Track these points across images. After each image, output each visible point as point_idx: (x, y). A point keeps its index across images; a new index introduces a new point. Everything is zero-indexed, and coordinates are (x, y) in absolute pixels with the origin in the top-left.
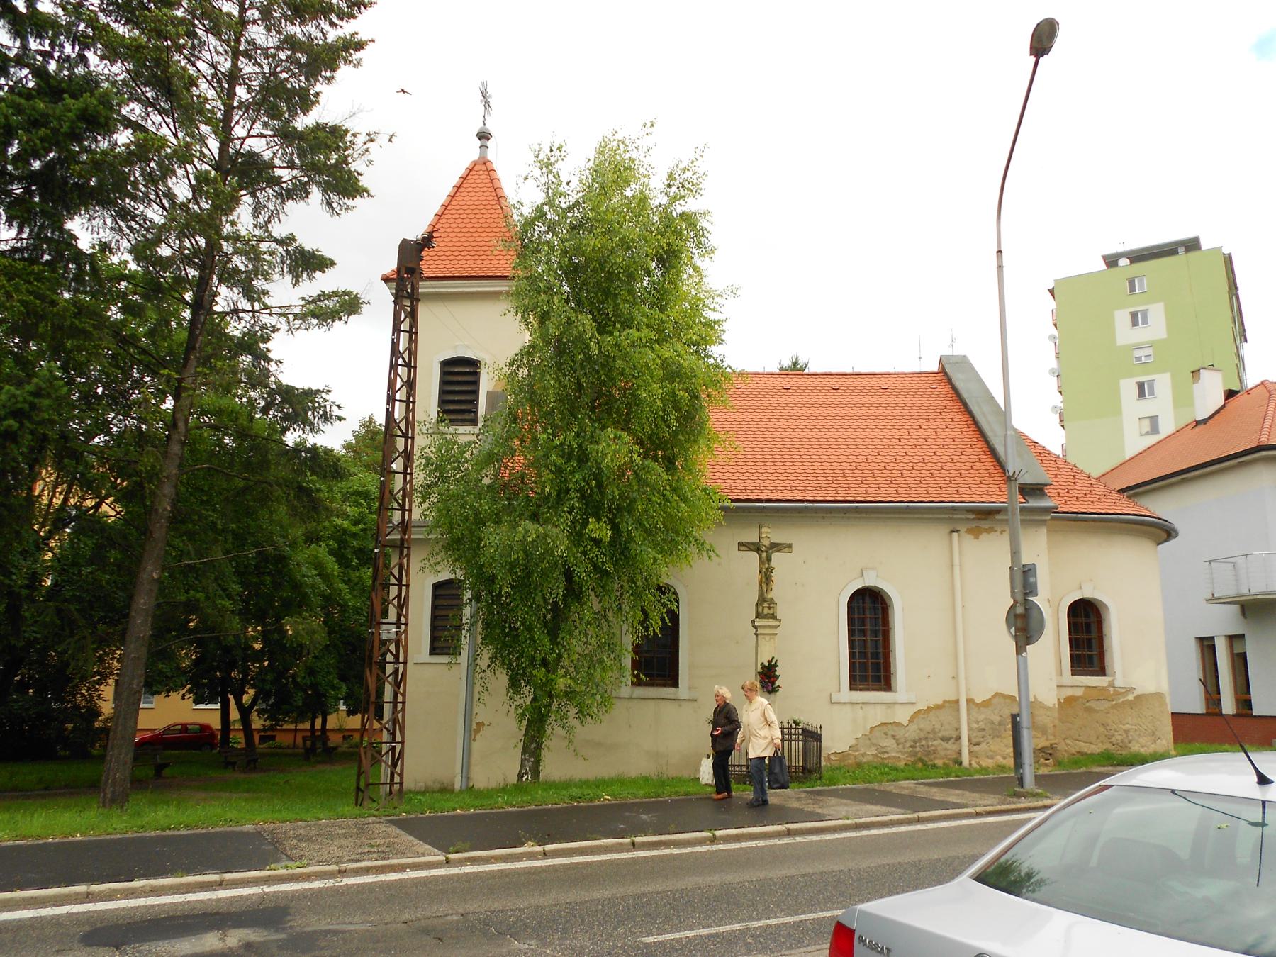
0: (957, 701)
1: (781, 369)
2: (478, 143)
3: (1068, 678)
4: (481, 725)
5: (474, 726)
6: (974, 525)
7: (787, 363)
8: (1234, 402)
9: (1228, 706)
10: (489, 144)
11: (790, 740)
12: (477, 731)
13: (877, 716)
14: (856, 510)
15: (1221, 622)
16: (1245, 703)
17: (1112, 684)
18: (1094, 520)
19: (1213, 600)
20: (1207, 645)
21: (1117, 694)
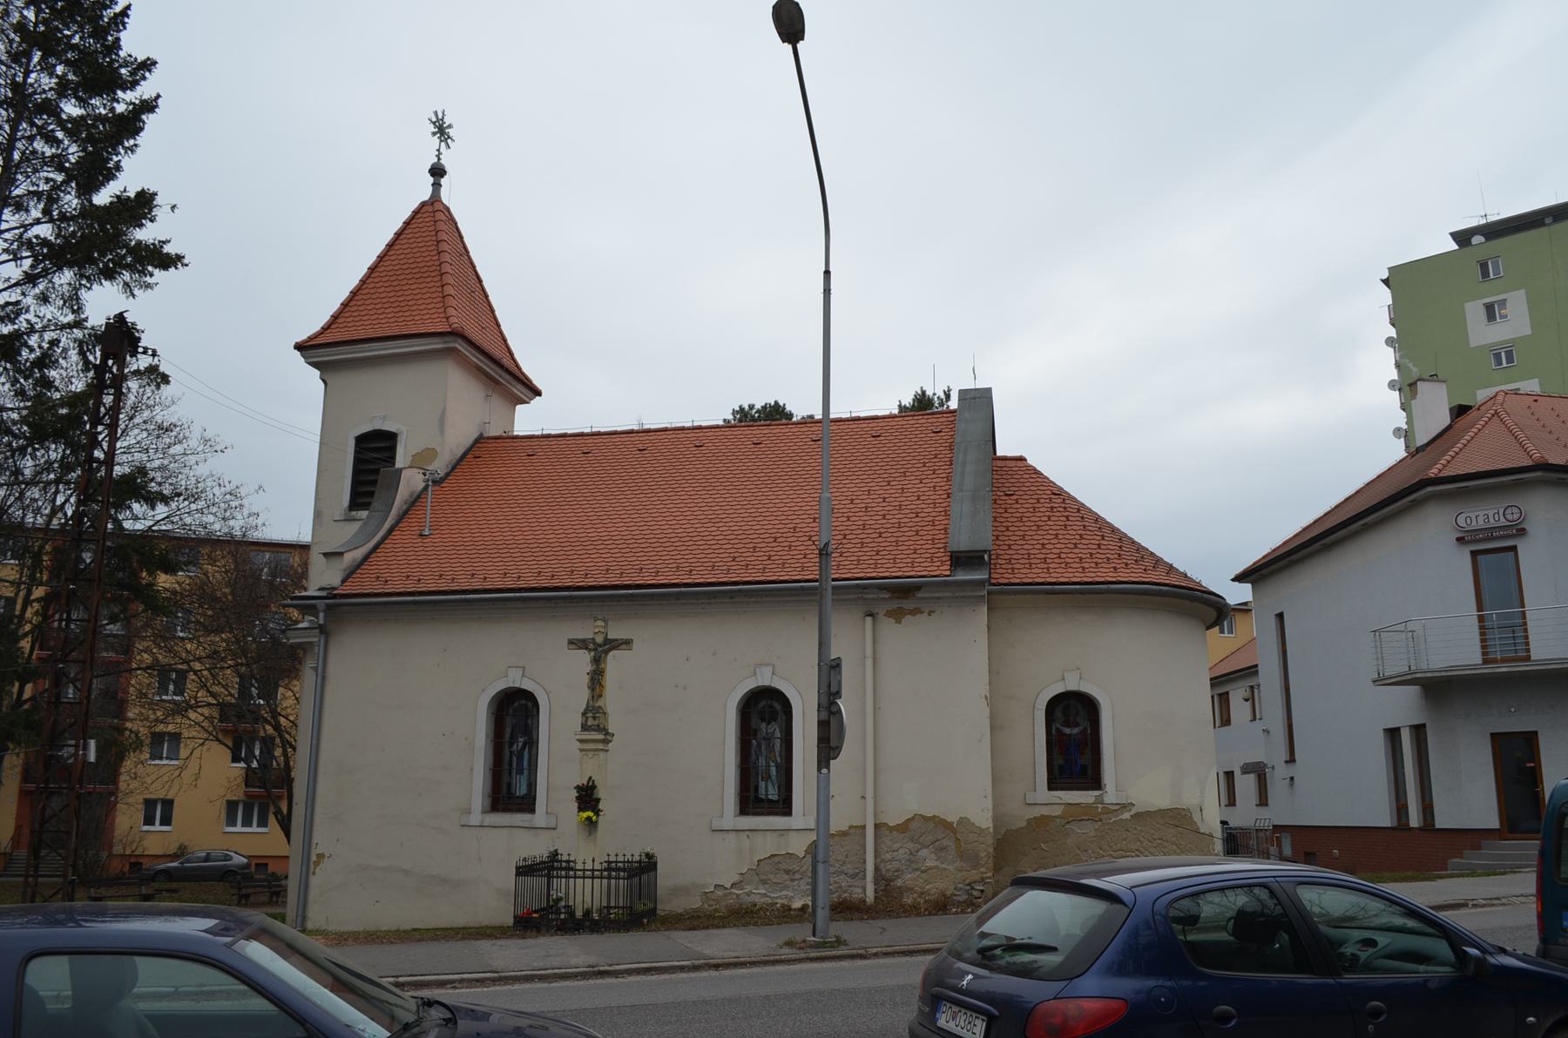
0: (864, 827)
1: (902, 408)
2: (431, 180)
3: (1043, 793)
4: (320, 856)
5: (314, 858)
6: (895, 605)
7: (908, 401)
8: (1466, 419)
9: (1415, 820)
10: (443, 181)
11: (609, 878)
12: (317, 863)
13: (767, 846)
14: (679, 596)
15: (1403, 707)
16: (1427, 809)
17: (1099, 800)
18: (1081, 592)
19: (1381, 681)
20: (1393, 734)
21: (1107, 811)
